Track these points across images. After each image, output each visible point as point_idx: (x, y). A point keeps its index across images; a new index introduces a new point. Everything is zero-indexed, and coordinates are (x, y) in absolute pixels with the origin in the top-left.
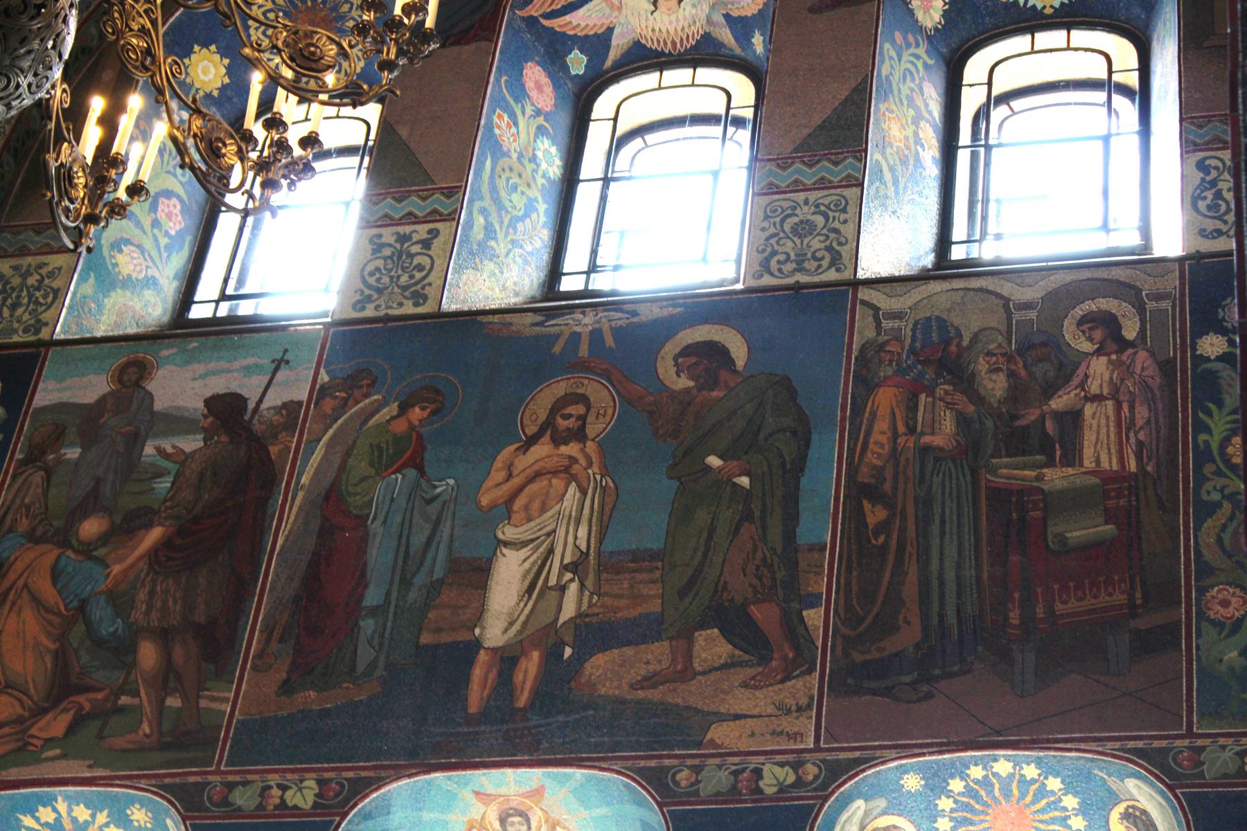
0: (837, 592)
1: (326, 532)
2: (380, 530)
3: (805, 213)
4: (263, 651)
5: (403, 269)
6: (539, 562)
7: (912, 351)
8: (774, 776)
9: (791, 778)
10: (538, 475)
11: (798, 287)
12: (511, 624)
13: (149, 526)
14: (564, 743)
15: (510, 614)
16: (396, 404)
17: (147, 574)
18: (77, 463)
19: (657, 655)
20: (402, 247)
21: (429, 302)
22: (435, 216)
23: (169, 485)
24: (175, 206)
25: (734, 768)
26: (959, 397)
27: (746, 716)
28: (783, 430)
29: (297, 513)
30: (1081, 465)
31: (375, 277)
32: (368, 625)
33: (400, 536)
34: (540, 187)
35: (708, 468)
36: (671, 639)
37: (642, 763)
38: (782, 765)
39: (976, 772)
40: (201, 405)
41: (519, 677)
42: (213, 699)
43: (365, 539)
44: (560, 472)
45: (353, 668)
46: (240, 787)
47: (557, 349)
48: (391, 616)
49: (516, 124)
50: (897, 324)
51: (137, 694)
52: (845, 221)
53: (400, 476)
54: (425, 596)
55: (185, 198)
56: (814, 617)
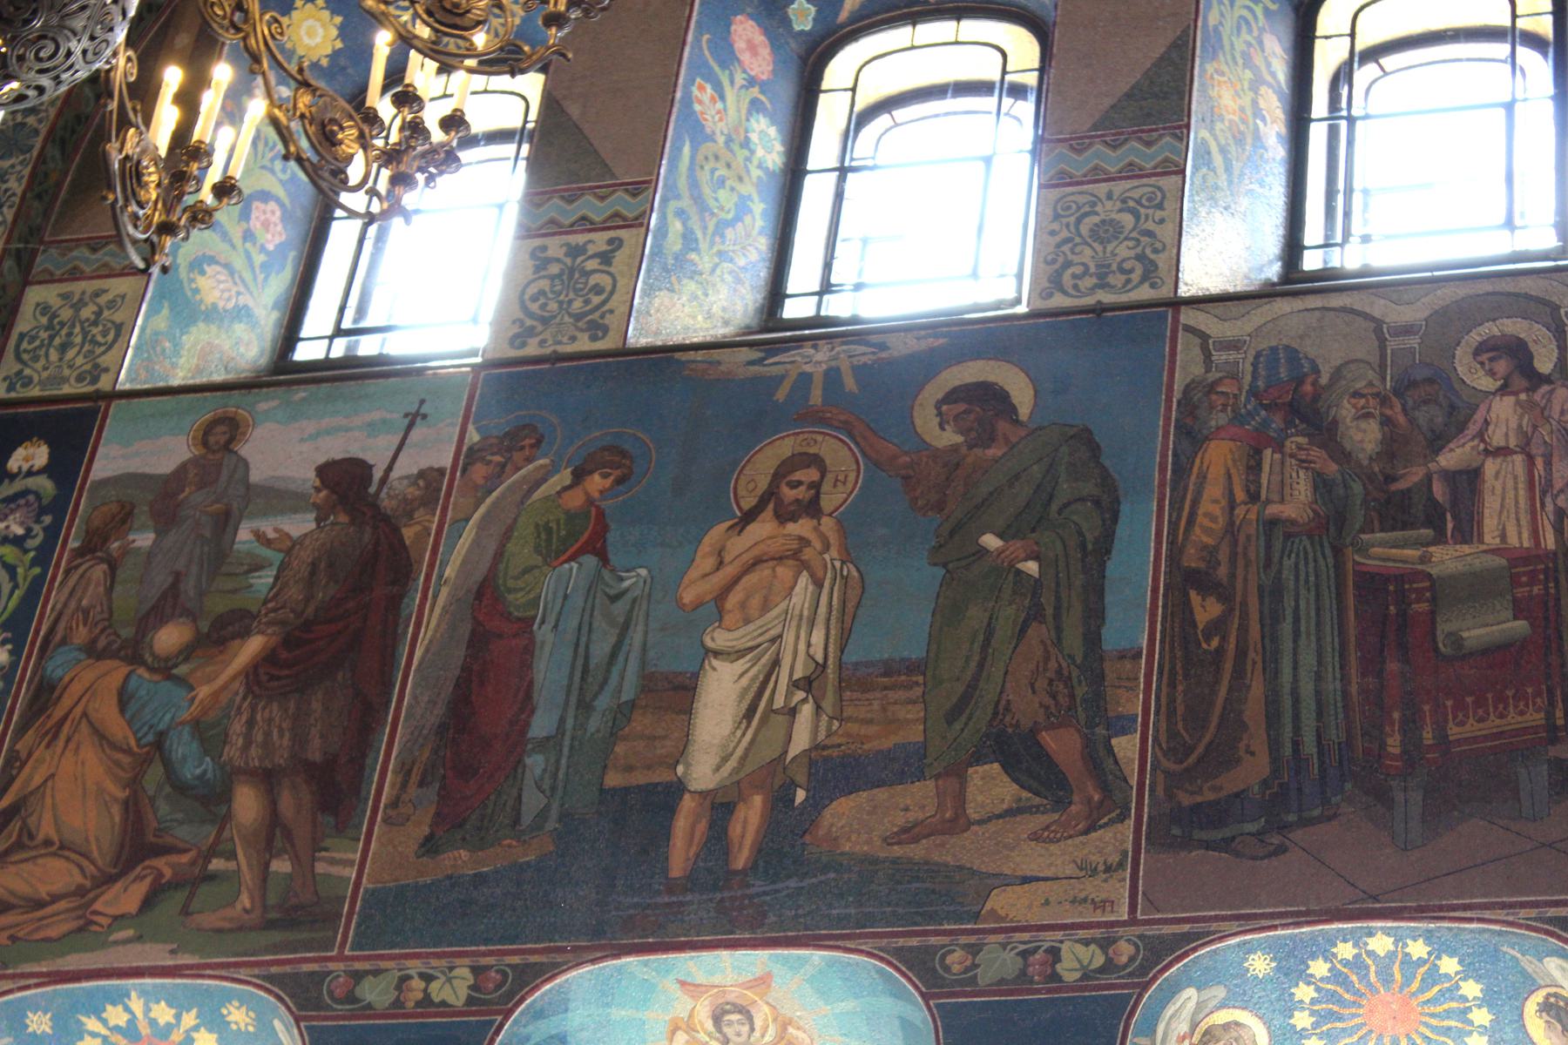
0: (1157, 713)
1: (479, 640)
2: (550, 637)
3: (1107, 210)
4: (398, 798)
5: (576, 291)
6: (761, 678)
7: (1254, 392)
8: (1076, 958)
9: (1099, 960)
10: (757, 562)
11: (1099, 310)
12: (725, 760)
13: (245, 634)
14: (797, 916)
15: (724, 746)
16: (569, 470)
17: (244, 698)
18: (150, 555)
20: (574, 262)
21: (611, 333)
22: (618, 221)
23: (271, 580)
24: (273, 212)
25: (1022, 947)
26: (1316, 453)
27: (1038, 879)
28: (1082, 499)
29: (441, 615)
30: (1481, 541)
32: (535, 763)
33: (577, 645)
34: (755, 180)
35: (983, 551)
36: (937, 777)
37: (901, 942)
38: (1086, 943)
39: (1345, 951)
40: (312, 474)
41: (735, 829)
42: (333, 862)
43: (529, 650)
44: (787, 557)
45: (516, 821)
46: (371, 978)
47: (781, 395)
48: (566, 751)
49: (722, 98)
50: (1232, 356)
51: (232, 855)
52: (1162, 221)
53: (575, 565)
54: (610, 724)
55: (287, 201)
56: (1126, 747)
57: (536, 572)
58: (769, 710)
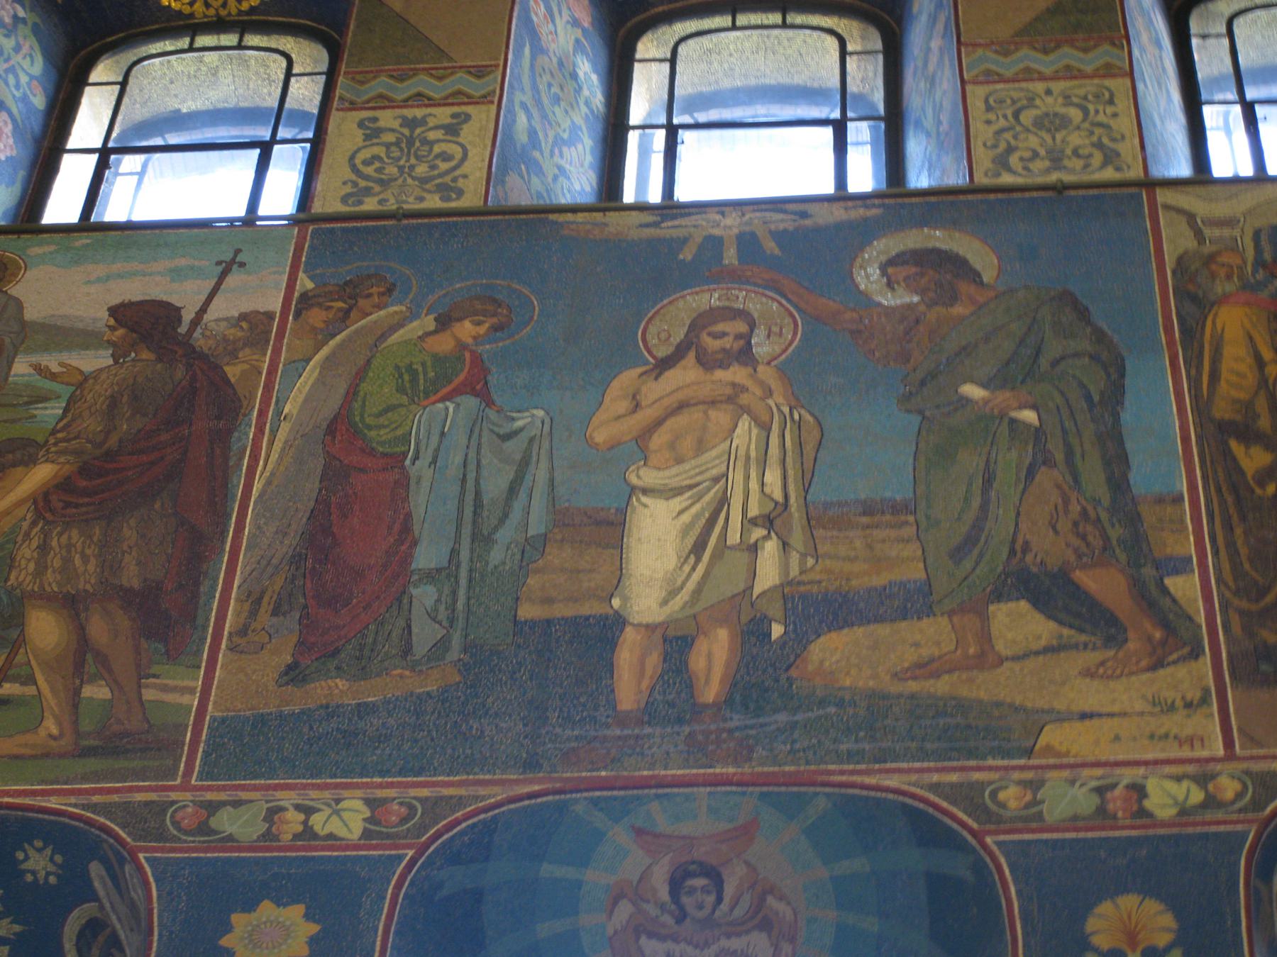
0: (1216, 553)
1: (334, 474)
7: (1259, 263)
9: (1197, 796)
10: (682, 406)
12: (673, 593)
17: (34, 524)
20: (412, 132)
25: (1094, 784)
27: (1100, 715)
28: (1076, 355)
29: (283, 449)
31: (374, 167)
32: (424, 595)
33: (464, 480)
35: (966, 401)
37: (935, 778)
38: (1179, 779)
41: (697, 662)
42: (165, 689)
43: (403, 483)
45: (407, 650)
46: (229, 808)
47: (687, 254)
48: (463, 581)
49: (553, 21)
50: (1226, 232)
51: (30, 680)
52: (1115, 115)
53: (451, 406)
54: (518, 557)
56: (1186, 588)
57: (403, 411)
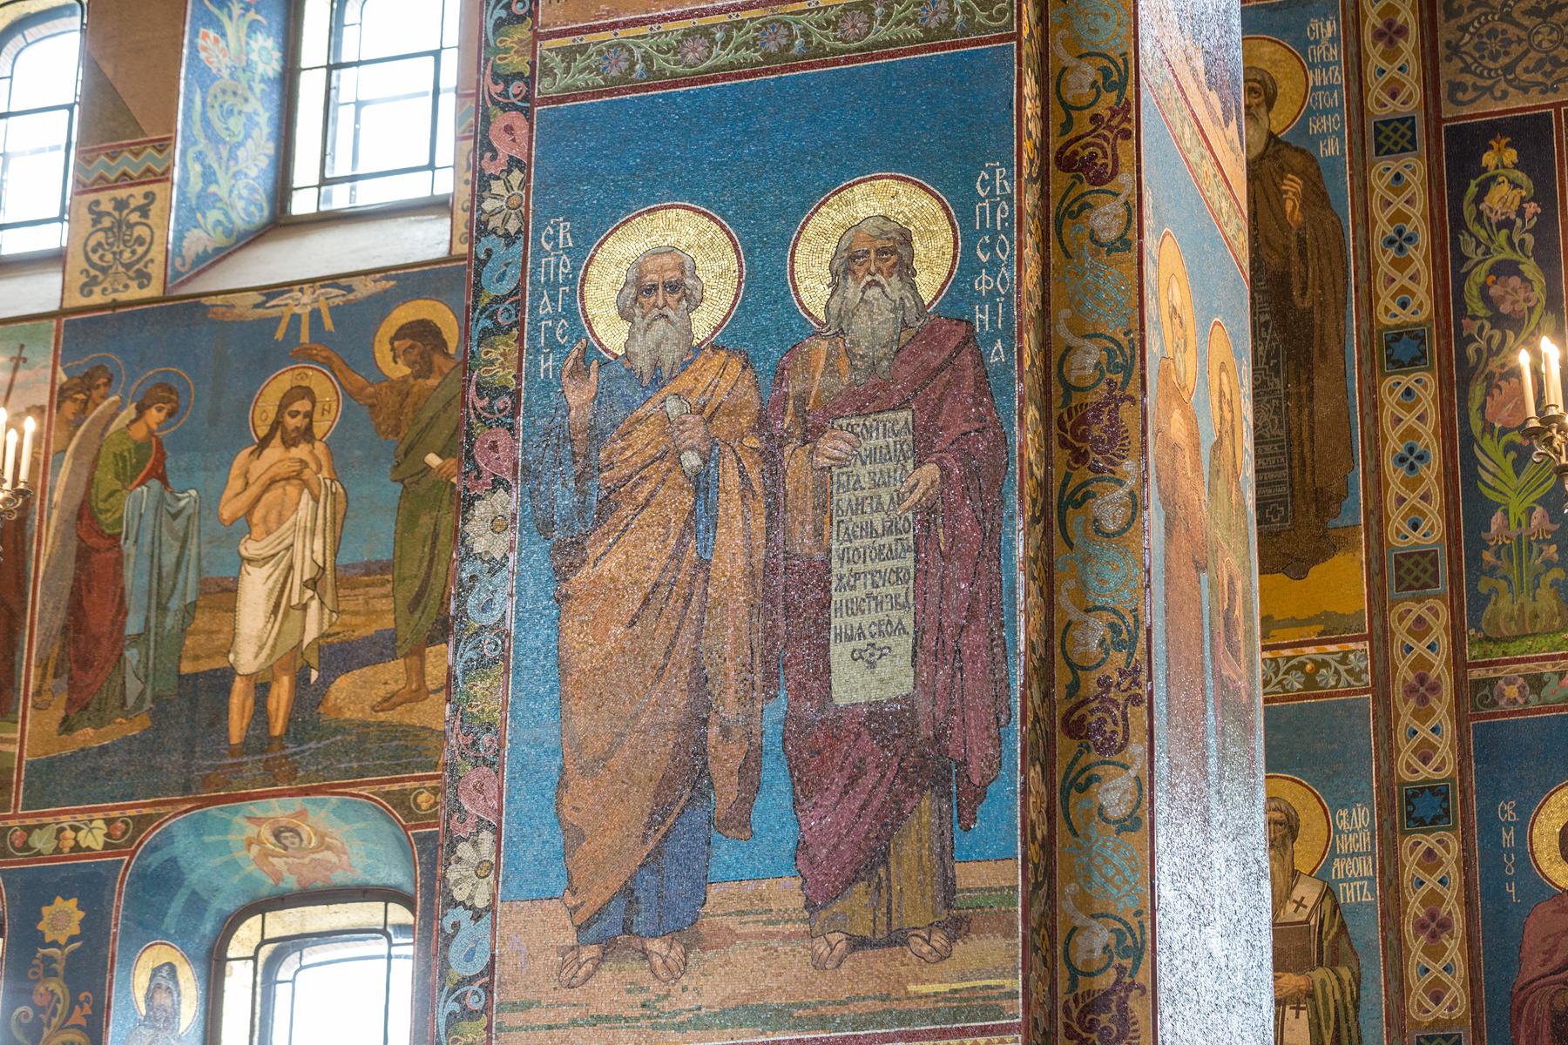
1: (84, 555)
2: (132, 551)
4: (40, 686)
5: (125, 242)
6: (282, 580)
10: (273, 482)
12: (261, 648)
14: (318, 770)
15: (260, 637)
16: (134, 405)
19: (392, 673)
21: (154, 282)
31: (98, 254)
32: (132, 655)
33: (152, 556)
34: (258, 95)
35: (428, 468)
36: (405, 656)
37: (387, 787)
41: (272, 704)
43: (119, 562)
44: (293, 477)
45: (124, 704)
47: (279, 335)
48: (152, 644)
49: (224, 35)
57: (118, 494)
58: (290, 607)
